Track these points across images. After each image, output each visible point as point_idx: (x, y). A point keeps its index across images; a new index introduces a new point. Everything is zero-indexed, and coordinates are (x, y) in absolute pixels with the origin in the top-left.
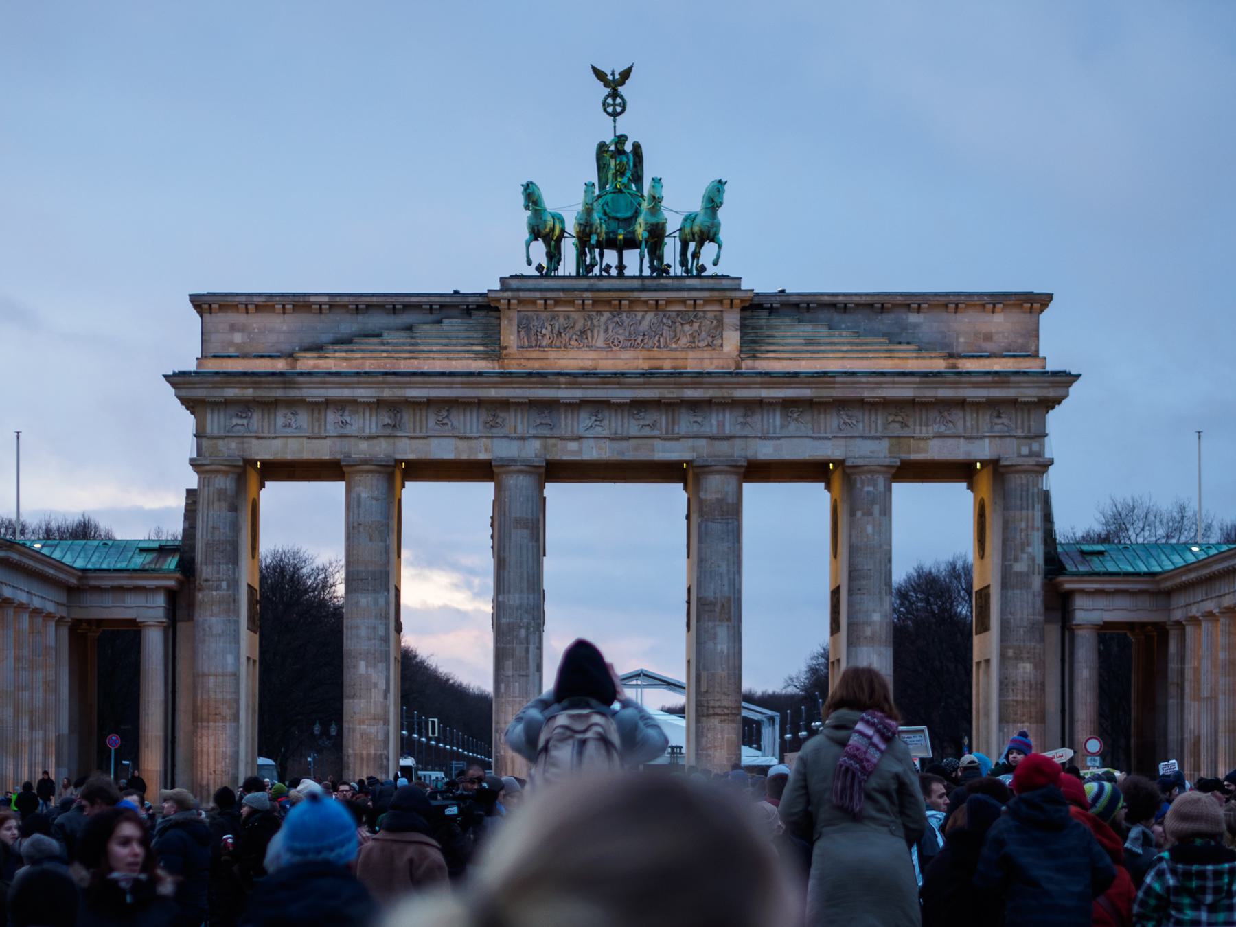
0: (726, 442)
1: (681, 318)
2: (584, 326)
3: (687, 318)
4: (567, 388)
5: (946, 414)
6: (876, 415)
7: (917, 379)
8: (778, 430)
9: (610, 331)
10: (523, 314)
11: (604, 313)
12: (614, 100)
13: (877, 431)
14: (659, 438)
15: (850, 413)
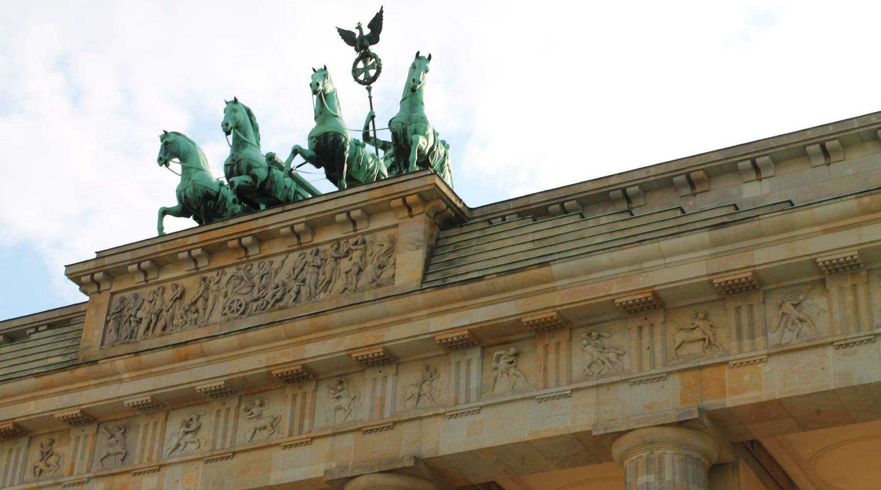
0: (386, 435)
1: (337, 249)
2: (198, 292)
3: (345, 246)
4: (132, 379)
5: (788, 307)
6: (652, 335)
7: (705, 236)
8: (473, 397)
9: (229, 294)
10: (117, 297)
11: (227, 270)
12: (365, 62)
13: (653, 367)
14: (278, 444)
15: (606, 342)
